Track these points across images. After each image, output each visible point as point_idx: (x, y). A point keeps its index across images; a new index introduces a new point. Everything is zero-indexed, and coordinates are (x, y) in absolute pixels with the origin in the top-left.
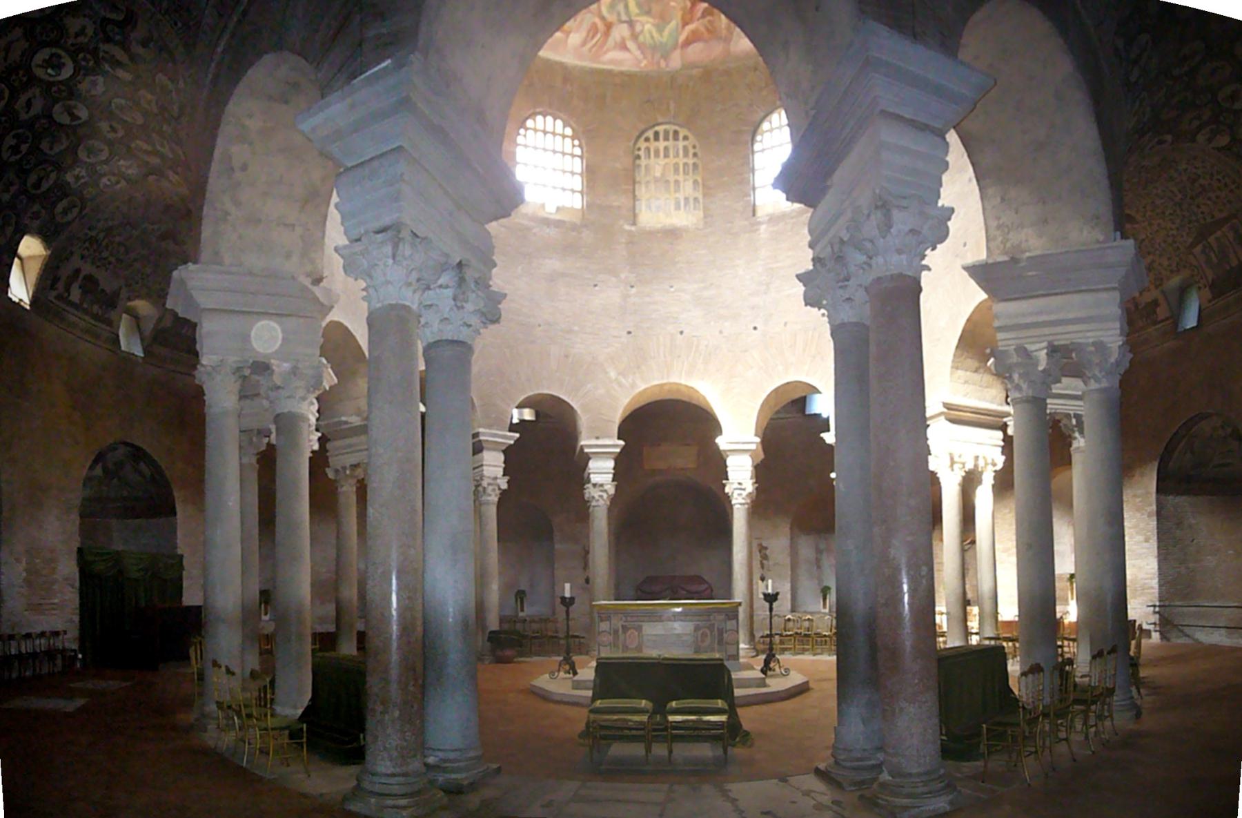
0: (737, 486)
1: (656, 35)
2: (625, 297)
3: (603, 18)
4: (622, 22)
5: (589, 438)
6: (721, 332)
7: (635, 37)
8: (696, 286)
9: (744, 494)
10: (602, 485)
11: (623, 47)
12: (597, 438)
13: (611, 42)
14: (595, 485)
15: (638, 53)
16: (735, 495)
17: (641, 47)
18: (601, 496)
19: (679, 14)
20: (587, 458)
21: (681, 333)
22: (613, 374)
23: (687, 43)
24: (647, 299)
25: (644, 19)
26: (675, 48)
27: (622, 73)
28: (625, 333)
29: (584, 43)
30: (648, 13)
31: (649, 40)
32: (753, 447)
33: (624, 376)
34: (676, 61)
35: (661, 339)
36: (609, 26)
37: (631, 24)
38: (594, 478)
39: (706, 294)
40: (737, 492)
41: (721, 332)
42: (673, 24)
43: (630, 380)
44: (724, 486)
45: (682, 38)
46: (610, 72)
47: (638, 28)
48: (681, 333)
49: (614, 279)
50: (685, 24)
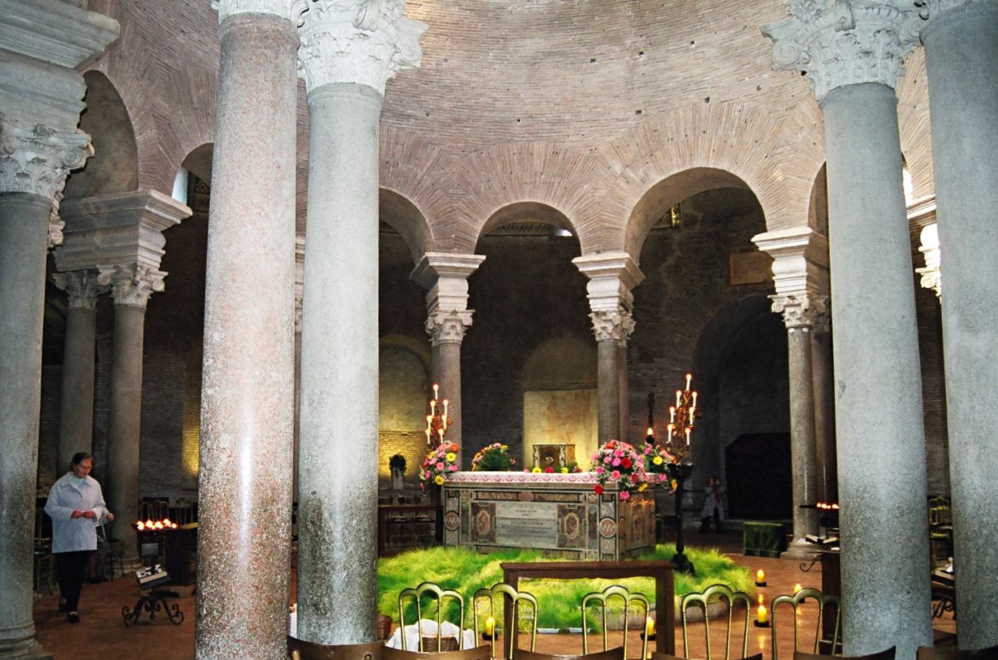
0: (787, 301)
2: (632, 69)
5: (588, 252)
6: (759, 89)
8: (724, 34)
9: (799, 311)
10: (604, 314)
12: (598, 252)
14: (597, 314)
16: (787, 316)
18: (604, 328)
20: (584, 279)
21: (708, 100)
22: (618, 168)
24: (662, 65)
28: (632, 114)
32: (806, 242)
33: (634, 170)
35: (681, 112)
38: (595, 305)
39: (738, 41)
40: (788, 310)
41: (759, 89)
43: (641, 172)
44: (771, 302)
48: (708, 100)
49: (617, 49)
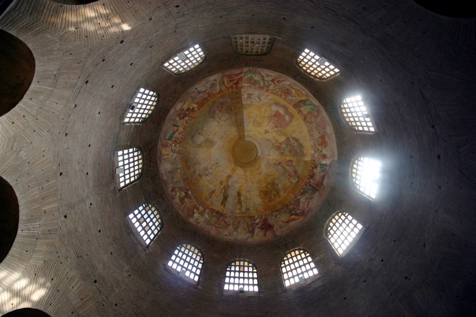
1: (254, 76)
3: (274, 83)
4: (267, 81)
7: (262, 77)
11: (268, 76)
13: (273, 78)
15: (261, 72)
17: (259, 73)
19: (243, 79)
23: (240, 73)
25: (258, 80)
26: (245, 72)
27: (270, 69)
29: (284, 81)
30: (255, 81)
31: (257, 75)
34: (245, 69)
36: (273, 81)
37: (263, 80)
42: (246, 77)
45: (242, 75)
46: (275, 70)
47: (261, 78)
50: (241, 78)
